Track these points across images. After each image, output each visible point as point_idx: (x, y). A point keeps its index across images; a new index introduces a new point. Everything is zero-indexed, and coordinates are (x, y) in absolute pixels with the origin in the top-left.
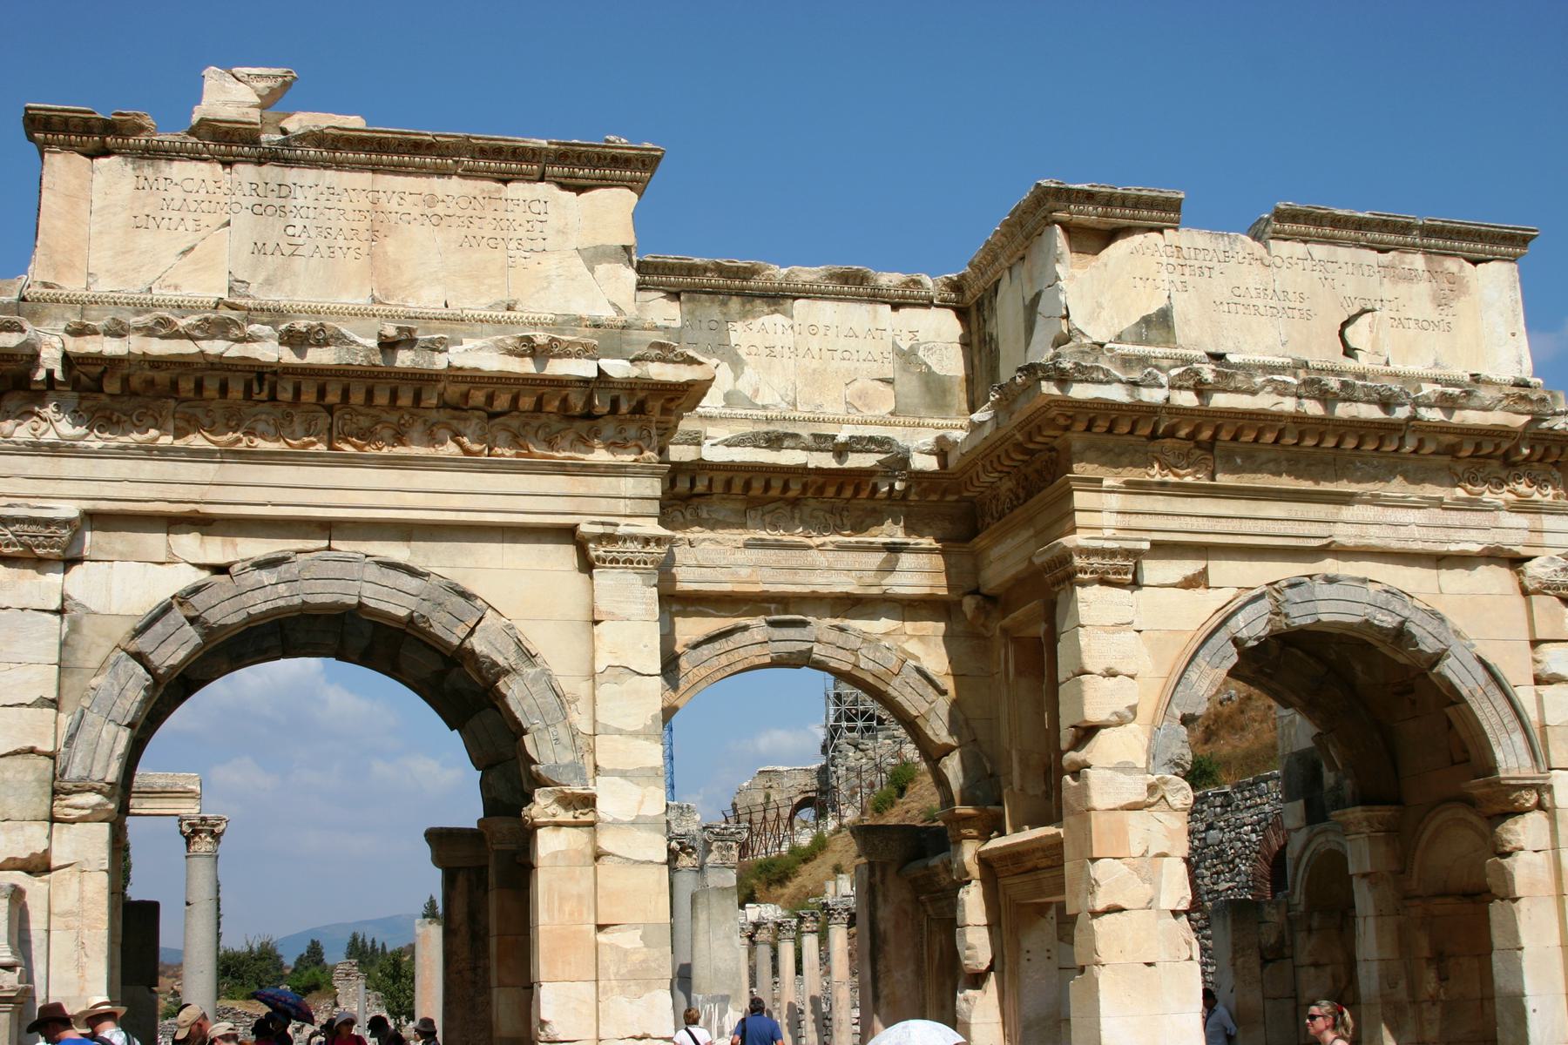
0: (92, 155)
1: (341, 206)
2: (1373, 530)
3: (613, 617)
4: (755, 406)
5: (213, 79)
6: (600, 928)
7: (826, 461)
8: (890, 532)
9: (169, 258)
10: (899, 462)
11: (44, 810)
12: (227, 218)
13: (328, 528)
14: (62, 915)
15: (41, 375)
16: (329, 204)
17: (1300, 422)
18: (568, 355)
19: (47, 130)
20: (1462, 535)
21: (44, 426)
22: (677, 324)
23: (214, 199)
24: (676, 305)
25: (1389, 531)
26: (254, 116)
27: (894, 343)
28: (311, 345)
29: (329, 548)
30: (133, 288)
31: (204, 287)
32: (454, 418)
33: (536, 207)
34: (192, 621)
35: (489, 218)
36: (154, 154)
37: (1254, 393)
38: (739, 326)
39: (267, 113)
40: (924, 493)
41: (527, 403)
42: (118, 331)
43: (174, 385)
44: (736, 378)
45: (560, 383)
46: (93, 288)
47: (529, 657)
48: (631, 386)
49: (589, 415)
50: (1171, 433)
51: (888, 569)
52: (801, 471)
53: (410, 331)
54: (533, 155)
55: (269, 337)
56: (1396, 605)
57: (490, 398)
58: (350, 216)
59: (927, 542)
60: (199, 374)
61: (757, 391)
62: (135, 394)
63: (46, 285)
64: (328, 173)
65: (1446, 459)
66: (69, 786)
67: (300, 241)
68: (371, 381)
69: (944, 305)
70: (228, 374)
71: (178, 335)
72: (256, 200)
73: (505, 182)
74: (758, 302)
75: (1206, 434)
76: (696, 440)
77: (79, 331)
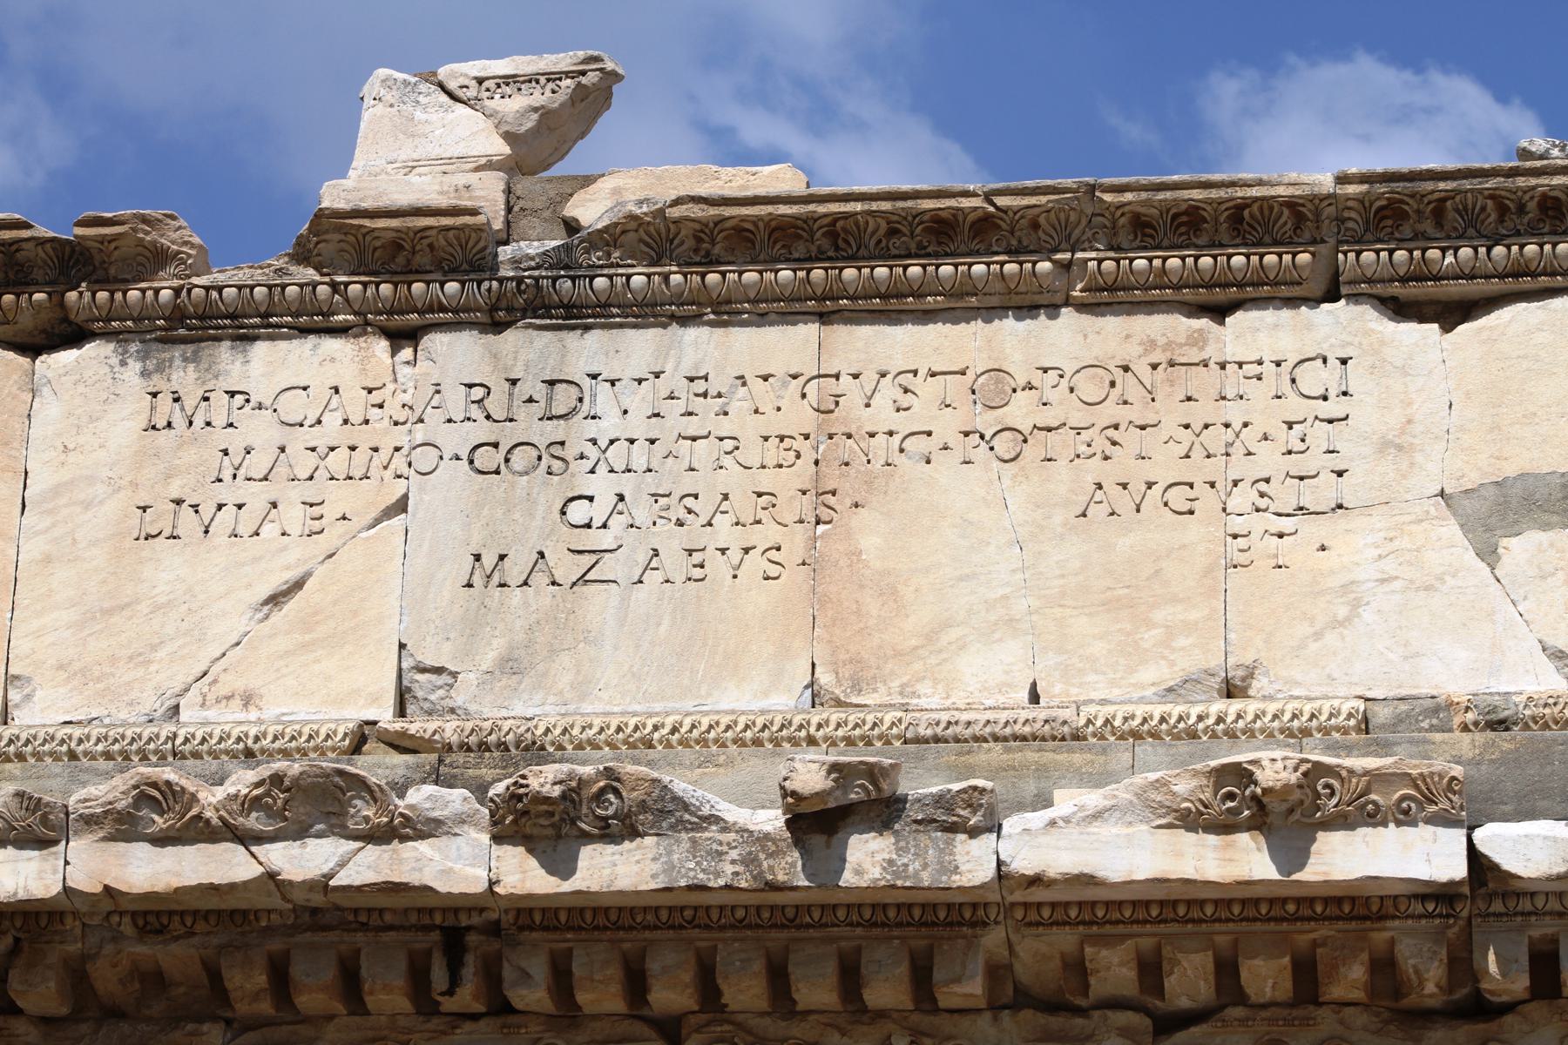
0: (32, 348)
1: (725, 427)
9: (232, 617)
12: (400, 488)
16: (692, 426)
18: (1374, 818)
23: (364, 438)
26: (488, 194)
28: (587, 838)
31: (322, 692)
33: (1314, 378)
35: (1170, 427)
39: (523, 185)
41: (1265, 976)
45: (1362, 906)
53: (872, 773)
54: (1295, 219)
55: (462, 820)
57: (1151, 970)
60: (276, 945)
62: (114, 1013)
64: (692, 334)
67: (605, 540)
70: (360, 937)
71: (199, 831)
73: (1220, 312)
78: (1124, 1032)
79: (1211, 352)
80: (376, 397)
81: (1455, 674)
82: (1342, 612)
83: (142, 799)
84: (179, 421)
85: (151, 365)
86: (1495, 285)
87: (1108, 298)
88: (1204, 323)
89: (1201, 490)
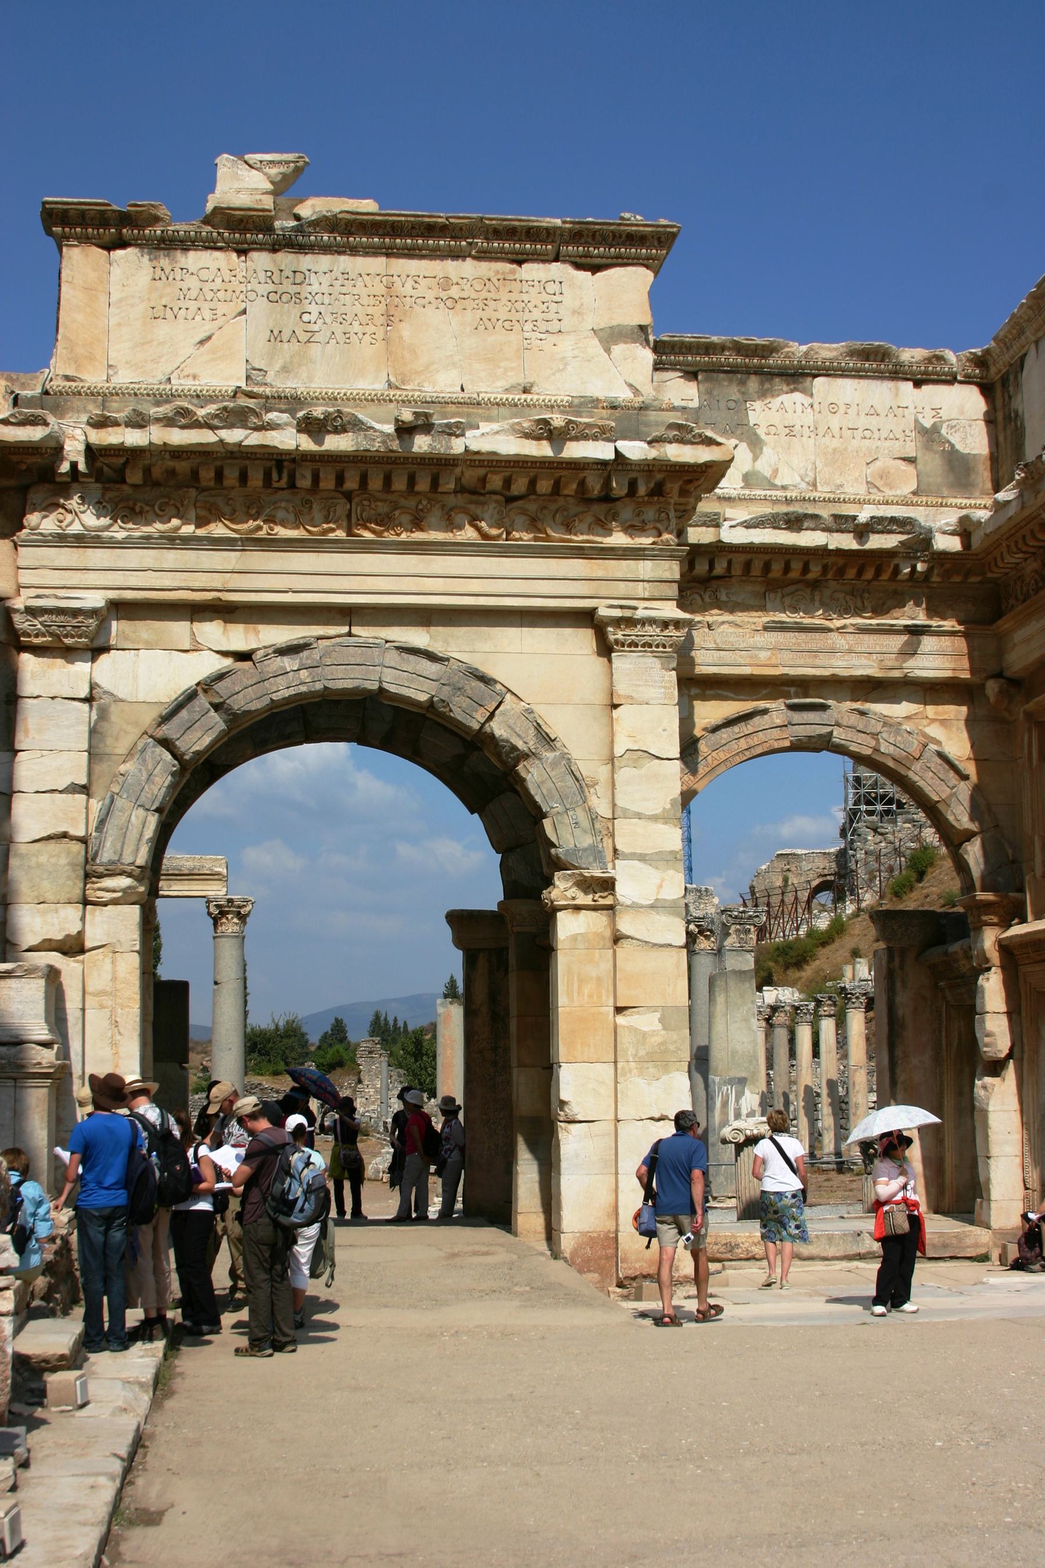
0: (109, 247)
1: (355, 291)
3: (632, 700)
4: (774, 487)
5: (226, 165)
6: (619, 1010)
7: (847, 542)
8: (913, 615)
9: (187, 348)
10: (920, 542)
11: (77, 893)
12: (243, 306)
13: (348, 614)
14: (96, 994)
15: (65, 467)
16: (344, 290)
18: (586, 438)
19: (67, 224)
21: (69, 517)
22: (695, 404)
24: (693, 385)
26: (268, 202)
27: (916, 421)
28: (329, 432)
29: (350, 634)
30: (152, 378)
31: (223, 376)
32: (471, 502)
33: (551, 288)
34: (217, 707)
35: (504, 301)
36: (170, 244)
38: (758, 405)
39: (281, 200)
40: (947, 574)
41: (544, 486)
42: (138, 422)
43: (195, 474)
44: (755, 458)
46: (114, 380)
47: (548, 741)
48: (649, 467)
49: (607, 498)
51: (910, 651)
52: (822, 552)
53: (427, 415)
54: (547, 235)
55: (287, 424)
57: (508, 482)
58: (365, 301)
59: (949, 624)
60: (218, 463)
61: (776, 471)
62: (157, 484)
63: (67, 378)
64: (343, 258)
66: (101, 869)
67: (316, 328)
68: (389, 467)
69: (968, 381)
70: (247, 462)
71: (197, 425)
72: (271, 287)
73: (520, 263)
74: (777, 380)
76: (715, 522)
77: (101, 423)
78: (496, 502)
79: (517, 276)
80: (233, 273)
81: (598, 389)
82: (561, 367)
83: (178, 413)
84: (164, 278)
85: (152, 257)
86: (610, 261)
87: (484, 256)
88: (514, 266)
89: (515, 322)
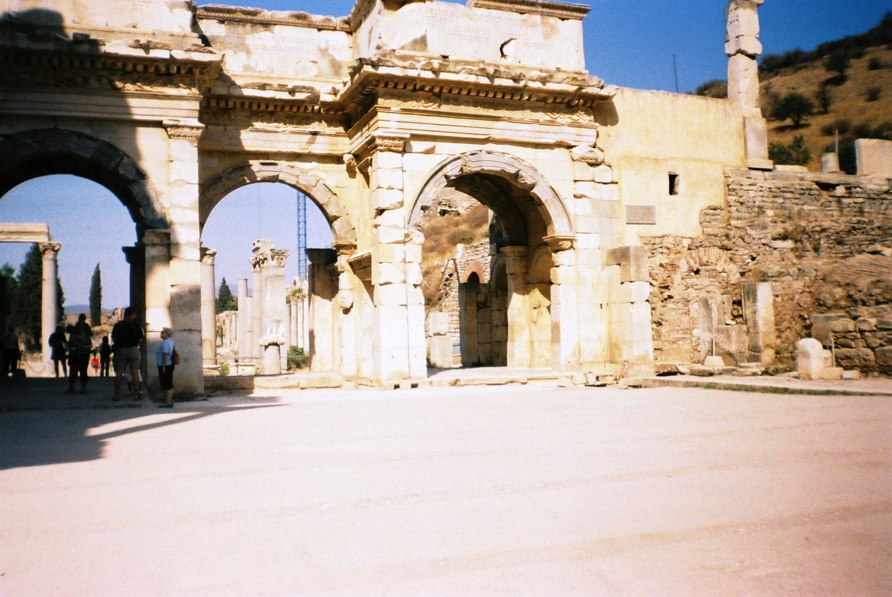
2: (508, 132)
4: (255, 71)
7: (286, 96)
8: (315, 126)
17: (479, 87)
20: (547, 135)
24: (223, 26)
25: (515, 133)
37: (457, 73)
38: (250, 36)
41: (140, 68)
49: (168, 74)
50: (422, 88)
51: (311, 142)
56: (516, 164)
65: (542, 104)
69: (342, 30)
75: (437, 90)
